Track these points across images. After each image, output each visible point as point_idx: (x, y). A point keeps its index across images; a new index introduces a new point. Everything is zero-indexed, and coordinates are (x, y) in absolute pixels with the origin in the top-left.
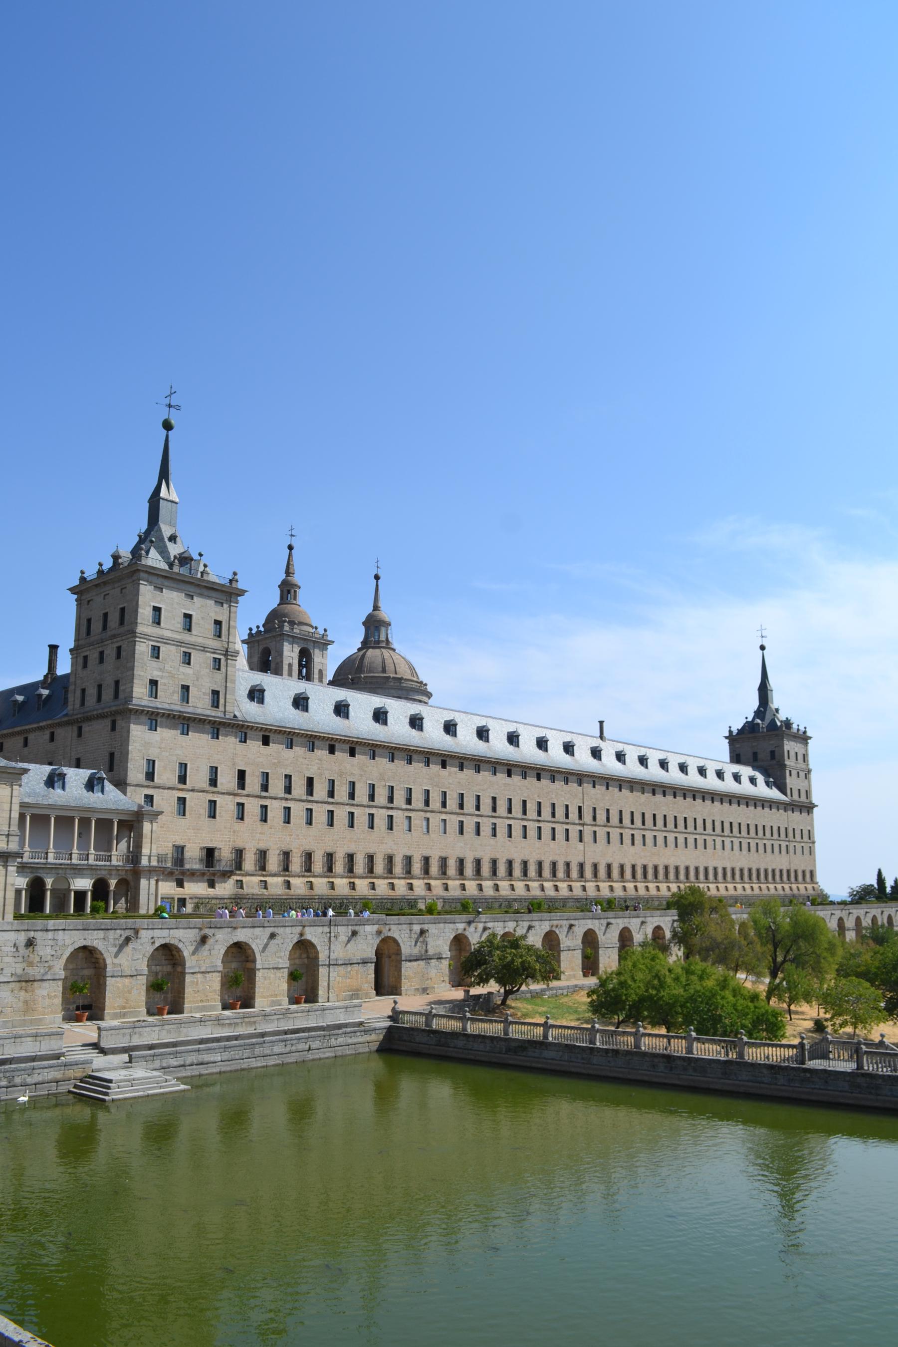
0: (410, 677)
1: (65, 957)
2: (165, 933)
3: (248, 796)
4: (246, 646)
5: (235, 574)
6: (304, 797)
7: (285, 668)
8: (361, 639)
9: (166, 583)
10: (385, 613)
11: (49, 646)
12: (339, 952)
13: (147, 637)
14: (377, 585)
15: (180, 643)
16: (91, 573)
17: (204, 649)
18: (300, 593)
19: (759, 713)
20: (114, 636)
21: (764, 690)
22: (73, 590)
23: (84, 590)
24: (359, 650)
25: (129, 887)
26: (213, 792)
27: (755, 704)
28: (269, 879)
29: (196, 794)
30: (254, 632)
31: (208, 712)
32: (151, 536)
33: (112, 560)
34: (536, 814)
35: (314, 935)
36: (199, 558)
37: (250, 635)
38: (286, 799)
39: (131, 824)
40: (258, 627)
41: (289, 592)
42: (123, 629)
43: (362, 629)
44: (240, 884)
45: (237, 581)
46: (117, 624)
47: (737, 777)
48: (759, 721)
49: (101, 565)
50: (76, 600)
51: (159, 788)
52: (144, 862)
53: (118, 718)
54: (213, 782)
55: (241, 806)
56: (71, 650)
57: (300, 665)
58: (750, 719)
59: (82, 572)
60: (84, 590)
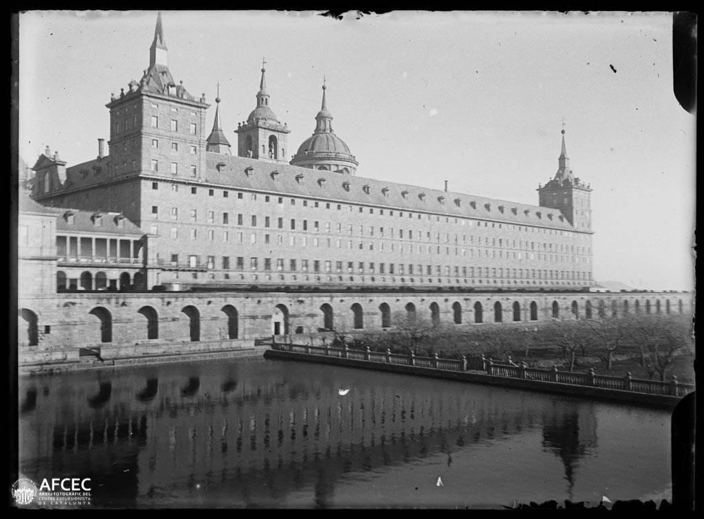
0: (344, 151)
2: (145, 300)
4: (237, 134)
5: (203, 95)
7: (261, 149)
8: (315, 129)
10: (330, 110)
11: (99, 140)
13: (149, 134)
14: (324, 93)
15: (171, 138)
16: (117, 96)
18: (270, 101)
19: (558, 175)
22: (107, 106)
23: (113, 105)
24: (313, 135)
25: (142, 276)
30: (241, 125)
32: (152, 70)
33: (129, 87)
34: (399, 236)
35: (232, 301)
36: (179, 84)
37: (239, 127)
38: (239, 228)
39: (142, 243)
40: (244, 122)
41: (262, 99)
43: (315, 121)
45: (204, 99)
47: (539, 214)
48: (558, 179)
49: (122, 90)
50: (110, 112)
52: (150, 262)
56: (109, 142)
57: (270, 146)
58: (552, 179)
59: (112, 95)
60: (113, 105)
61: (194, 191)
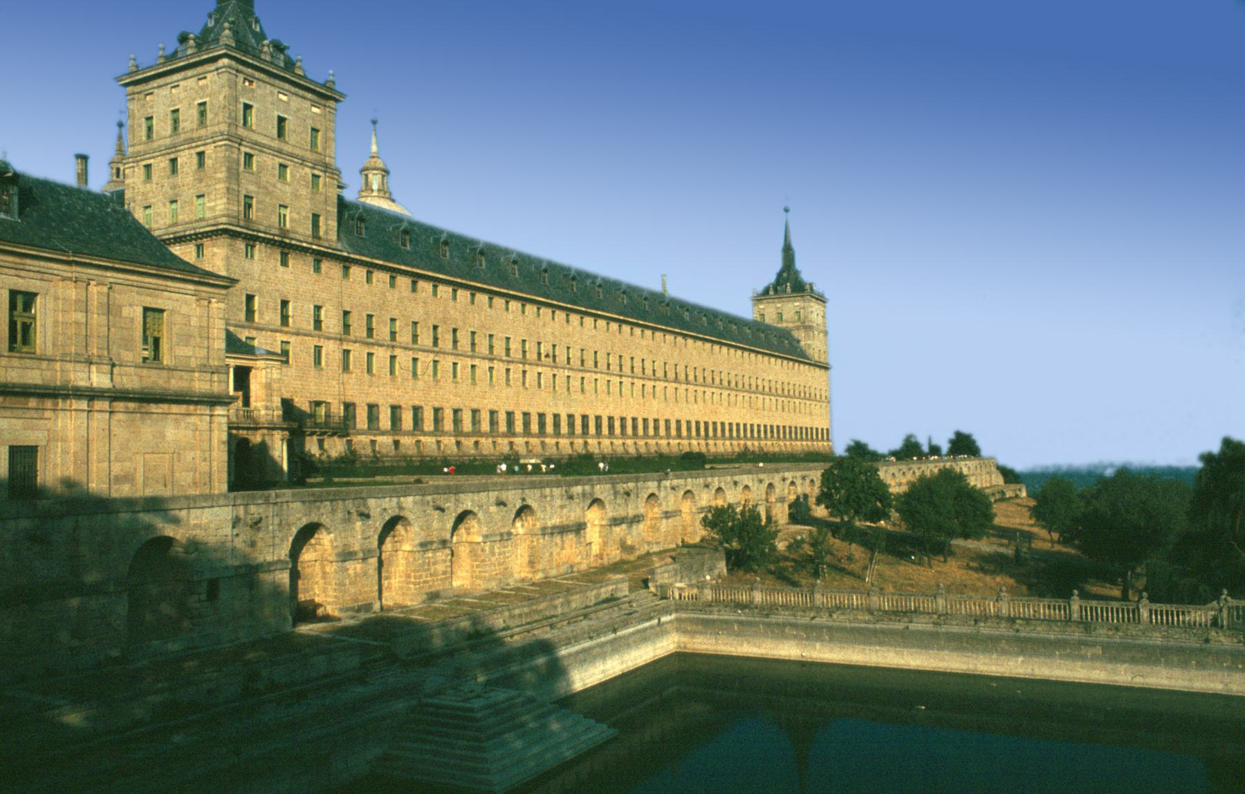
1: (291, 539)
3: (355, 342)
6: (410, 346)
9: (257, 74)
12: (556, 521)
17: (303, 161)
20: (193, 140)
21: (788, 252)
26: (319, 337)
27: (778, 265)
28: (380, 439)
29: (300, 338)
31: (310, 240)
42: (202, 132)
44: (349, 443)
46: (195, 126)
51: (262, 329)
53: (206, 242)
54: (318, 323)
55: (347, 352)
61: (317, 270)
